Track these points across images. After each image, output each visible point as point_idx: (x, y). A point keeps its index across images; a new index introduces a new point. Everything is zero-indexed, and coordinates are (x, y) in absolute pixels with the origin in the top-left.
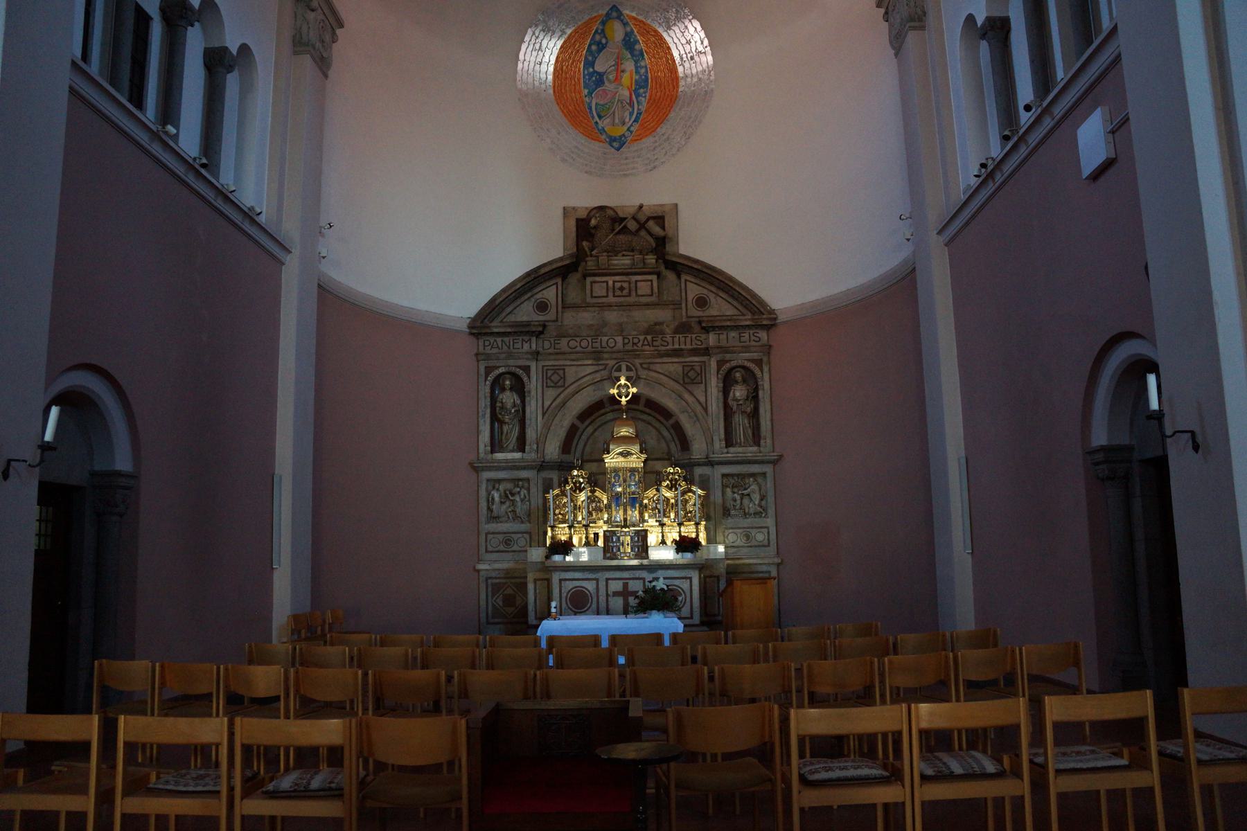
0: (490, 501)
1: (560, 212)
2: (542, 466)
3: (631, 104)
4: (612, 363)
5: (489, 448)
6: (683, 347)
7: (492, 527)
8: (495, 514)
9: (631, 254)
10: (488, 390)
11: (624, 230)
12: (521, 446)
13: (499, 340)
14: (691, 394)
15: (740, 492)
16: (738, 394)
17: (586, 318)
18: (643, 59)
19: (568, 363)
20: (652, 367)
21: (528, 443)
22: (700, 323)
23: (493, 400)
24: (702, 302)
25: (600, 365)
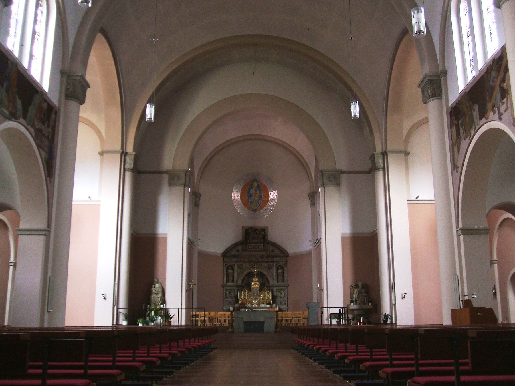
0: (226, 294)
1: (241, 228)
2: (238, 286)
3: (258, 201)
6: (268, 260)
7: (226, 299)
11: (256, 234)
12: (233, 282)
14: (270, 271)
17: (247, 253)
23: (227, 272)
24: (273, 251)
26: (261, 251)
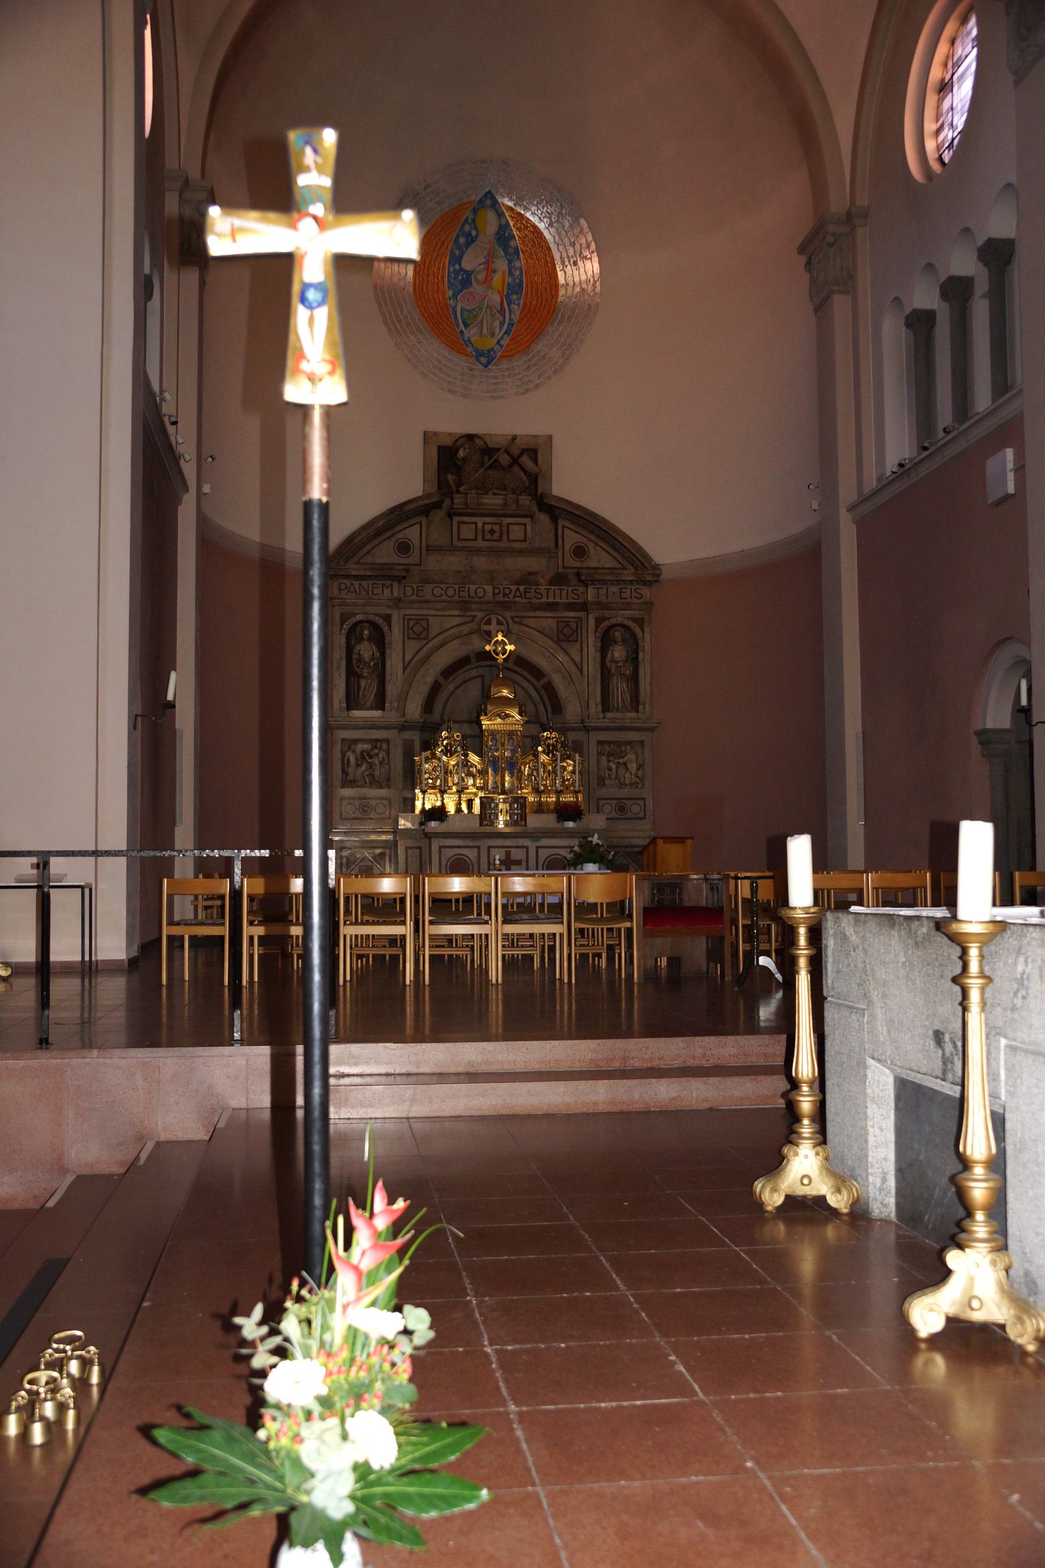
3: (502, 312)
4: (479, 615)
5: (344, 705)
6: (558, 600)
7: (347, 792)
8: (351, 777)
9: (504, 493)
10: (343, 640)
11: (496, 465)
13: (356, 583)
15: (616, 761)
16: (616, 655)
17: (453, 562)
18: (519, 258)
19: (433, 612)
20: (524, 621)
21: (388, 700)
22: (578, 575)
23: (349, 651)
24: (580, 552)
25: (468, 616)
26: (521, 552)
